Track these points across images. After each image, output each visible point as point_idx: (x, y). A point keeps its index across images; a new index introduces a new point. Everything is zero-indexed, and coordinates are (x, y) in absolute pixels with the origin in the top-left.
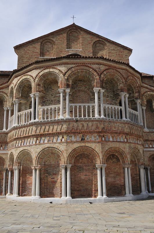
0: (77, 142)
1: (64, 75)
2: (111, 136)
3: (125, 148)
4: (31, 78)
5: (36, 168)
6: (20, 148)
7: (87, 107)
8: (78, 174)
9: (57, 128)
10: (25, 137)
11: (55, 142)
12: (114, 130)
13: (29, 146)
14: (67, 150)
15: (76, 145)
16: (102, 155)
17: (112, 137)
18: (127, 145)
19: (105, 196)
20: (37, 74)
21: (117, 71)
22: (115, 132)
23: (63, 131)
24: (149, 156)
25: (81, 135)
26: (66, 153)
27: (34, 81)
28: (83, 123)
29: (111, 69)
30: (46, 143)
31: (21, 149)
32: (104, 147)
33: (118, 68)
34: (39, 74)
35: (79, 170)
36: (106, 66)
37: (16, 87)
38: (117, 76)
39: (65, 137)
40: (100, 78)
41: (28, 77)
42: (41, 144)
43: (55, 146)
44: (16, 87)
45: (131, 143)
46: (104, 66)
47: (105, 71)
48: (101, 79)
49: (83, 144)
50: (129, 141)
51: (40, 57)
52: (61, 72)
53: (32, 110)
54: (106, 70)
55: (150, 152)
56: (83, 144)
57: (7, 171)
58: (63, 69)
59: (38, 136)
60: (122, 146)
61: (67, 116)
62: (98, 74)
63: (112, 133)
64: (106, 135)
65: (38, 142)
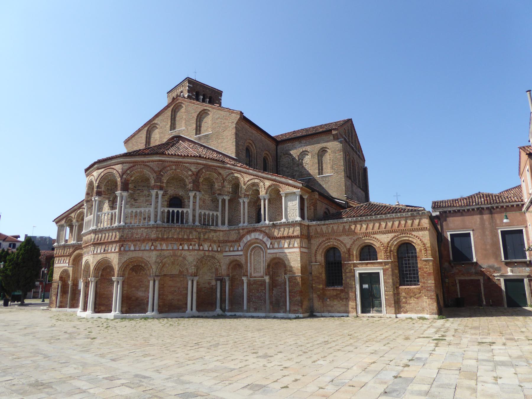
0: (101, 253)
2: (132, 245)
3: (150, 258)
7: (113, 213)
8: (109, 288)
12: (136, 238)
14: (93, 263)
15: (99, 257)
16: (118, 267)
17: (134, 245)
18: (154, 253)
21: (145, 165)
22: (137, 239)
24: (228, 263)
29: (137, 165)
32: (121, 257)
33: (147, 162)
35: (110, 283)
36: (131, 163)
38: (147, 172)
40: (121, 179)
45: (163, 250)
46: (127, 164)
47: (128, 169)
48: (123, 181)
49: (105, 256)
50: (159, 248)
54: (130, 168)
55: (230, 257)
56: (105, 256)
60: (146, 255)
63: (133, 241)
64: (125, 243)
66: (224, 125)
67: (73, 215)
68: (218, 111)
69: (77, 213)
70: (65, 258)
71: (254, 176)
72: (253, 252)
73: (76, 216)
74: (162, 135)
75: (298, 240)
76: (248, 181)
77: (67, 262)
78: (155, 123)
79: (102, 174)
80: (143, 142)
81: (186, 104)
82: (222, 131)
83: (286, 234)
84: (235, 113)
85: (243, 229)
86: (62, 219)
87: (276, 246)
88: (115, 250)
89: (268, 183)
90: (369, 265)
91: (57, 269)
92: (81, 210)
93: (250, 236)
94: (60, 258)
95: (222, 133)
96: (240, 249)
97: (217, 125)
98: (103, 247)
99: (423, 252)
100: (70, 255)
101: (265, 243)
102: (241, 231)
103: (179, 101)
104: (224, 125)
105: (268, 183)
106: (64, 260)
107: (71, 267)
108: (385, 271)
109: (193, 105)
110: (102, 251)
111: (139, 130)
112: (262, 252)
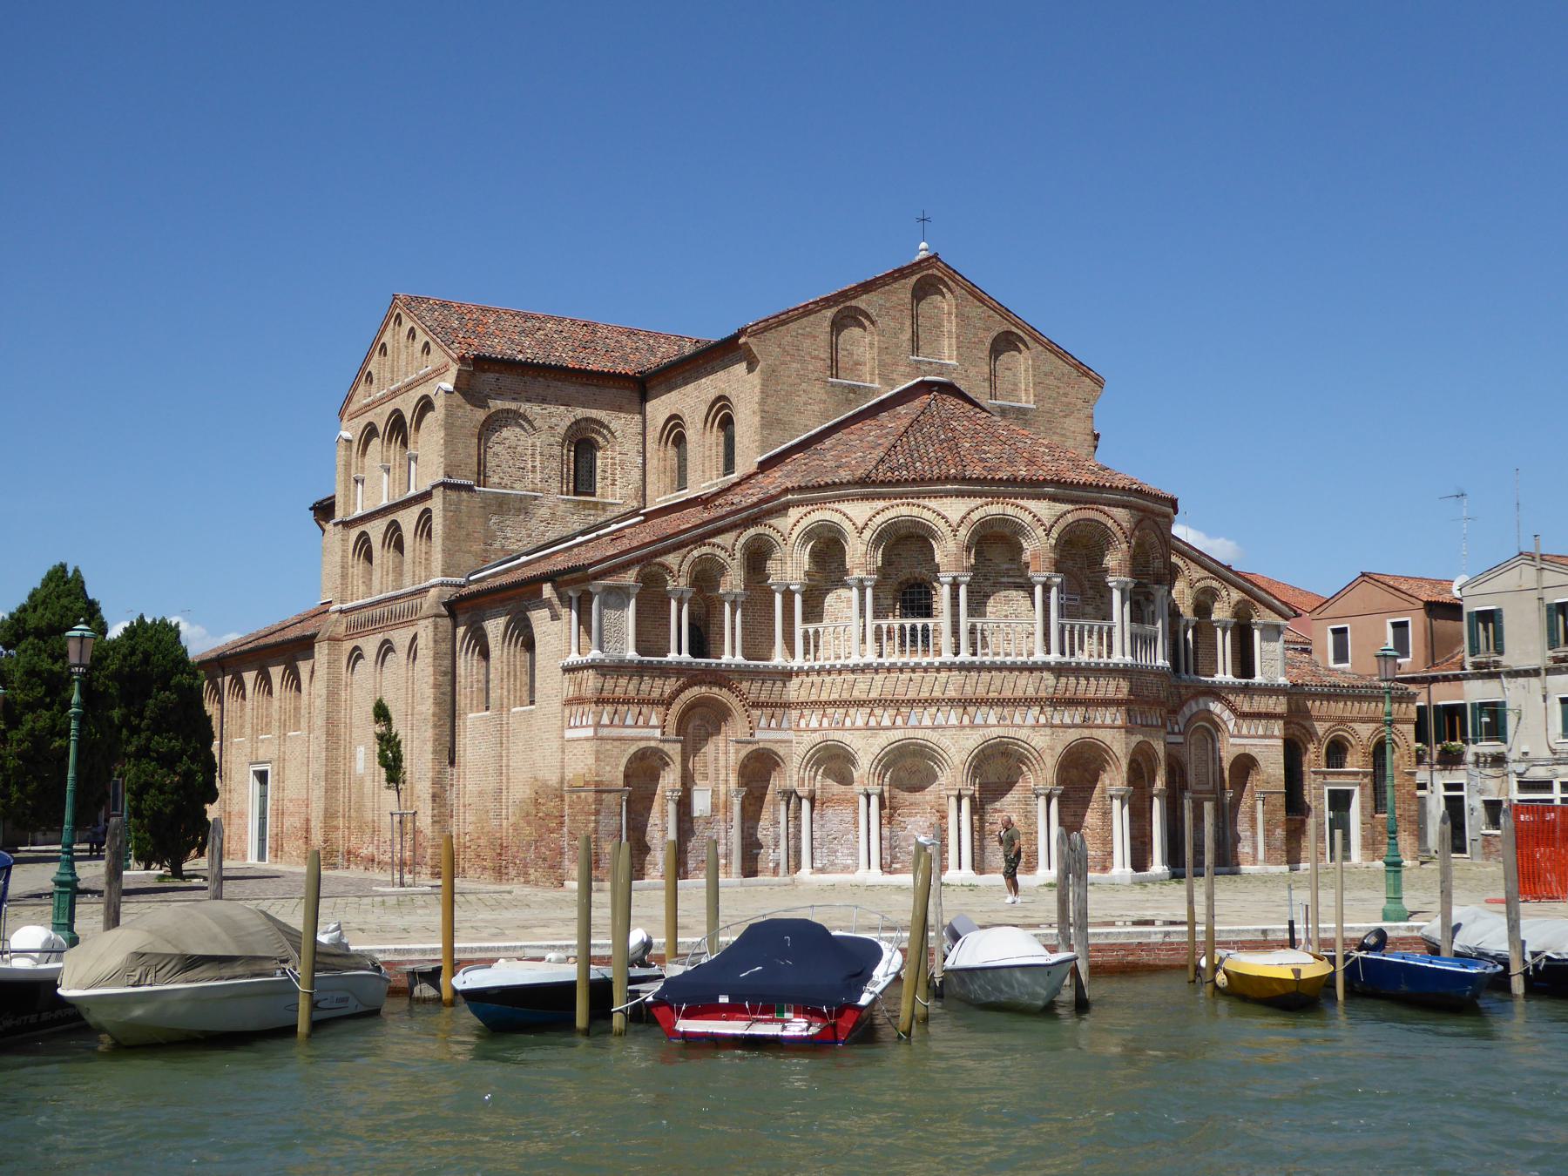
1: (1048, 532)
4: (941, 523)
5: (963, 792)
6: (890, 733)
9: (1026, 685)
10: (911, 703)
11: (1021, 723)
13: (934, 728)
15: (1073, 735)
19: (1129, 869)
20: (963, 513)
23: (1042, 694)
26: (1052, 756)
27: (955, 535)
30: (994, 726)
31: (897, 735)
34: (969, 514)
39: (1048, 710)
41: (927, 515)
42: (979, 726)
43: (1022, 734)
44: (867, 534)
49: (1086, 733)
51: (830, 379)
52: (1039, 520)
56: (1086, 733)
57: (788, 795)
58: (1044, 509)
59: (964, 703)
61: (1054, 657)
62: (1126, 537)
65: (966, 720)
66: (1064, 399)
67: (671, 560)
68: (1048, 353)
69: (690, 558)
70: (645, 710)
71: (1209, 571)
72: (1194, 737)
73: (685, 568)
74: (888, 359)
75: (1281, 723)
76: (1199, 581)
77: (654, 721)
78: (856, 309)
79: (1070, 518)
80: (822, 356)
81: (958, 290)
82: (1061, 414)
83: (1263, 710)
84: (1092, 379)
85: (1187, 687)
86: (625, 567)
87: (1245, 731)
88: (1113, 721)
89: (1236, 595)
90: (1341, 777)
91: (608, 747)
92: (705, 550)
93: (1197, 703)
94: (622, 708)
95: (1059, 420)
96: (1176, 730)
97: (1049, 393)
98: (1082, 710)
99: (1406, 759)
100: (667, 703)
101: (1225, 723)
102: (1183, 691)
103: (935, 272)
104: (1066, 400)
105: (1236, 595)
106: (640, 713)
107: (675, 741)
108: (1363, 787)
109: (978, 303)
110: (1078, 720)
111: (806, 311)
112: (1210, 741)
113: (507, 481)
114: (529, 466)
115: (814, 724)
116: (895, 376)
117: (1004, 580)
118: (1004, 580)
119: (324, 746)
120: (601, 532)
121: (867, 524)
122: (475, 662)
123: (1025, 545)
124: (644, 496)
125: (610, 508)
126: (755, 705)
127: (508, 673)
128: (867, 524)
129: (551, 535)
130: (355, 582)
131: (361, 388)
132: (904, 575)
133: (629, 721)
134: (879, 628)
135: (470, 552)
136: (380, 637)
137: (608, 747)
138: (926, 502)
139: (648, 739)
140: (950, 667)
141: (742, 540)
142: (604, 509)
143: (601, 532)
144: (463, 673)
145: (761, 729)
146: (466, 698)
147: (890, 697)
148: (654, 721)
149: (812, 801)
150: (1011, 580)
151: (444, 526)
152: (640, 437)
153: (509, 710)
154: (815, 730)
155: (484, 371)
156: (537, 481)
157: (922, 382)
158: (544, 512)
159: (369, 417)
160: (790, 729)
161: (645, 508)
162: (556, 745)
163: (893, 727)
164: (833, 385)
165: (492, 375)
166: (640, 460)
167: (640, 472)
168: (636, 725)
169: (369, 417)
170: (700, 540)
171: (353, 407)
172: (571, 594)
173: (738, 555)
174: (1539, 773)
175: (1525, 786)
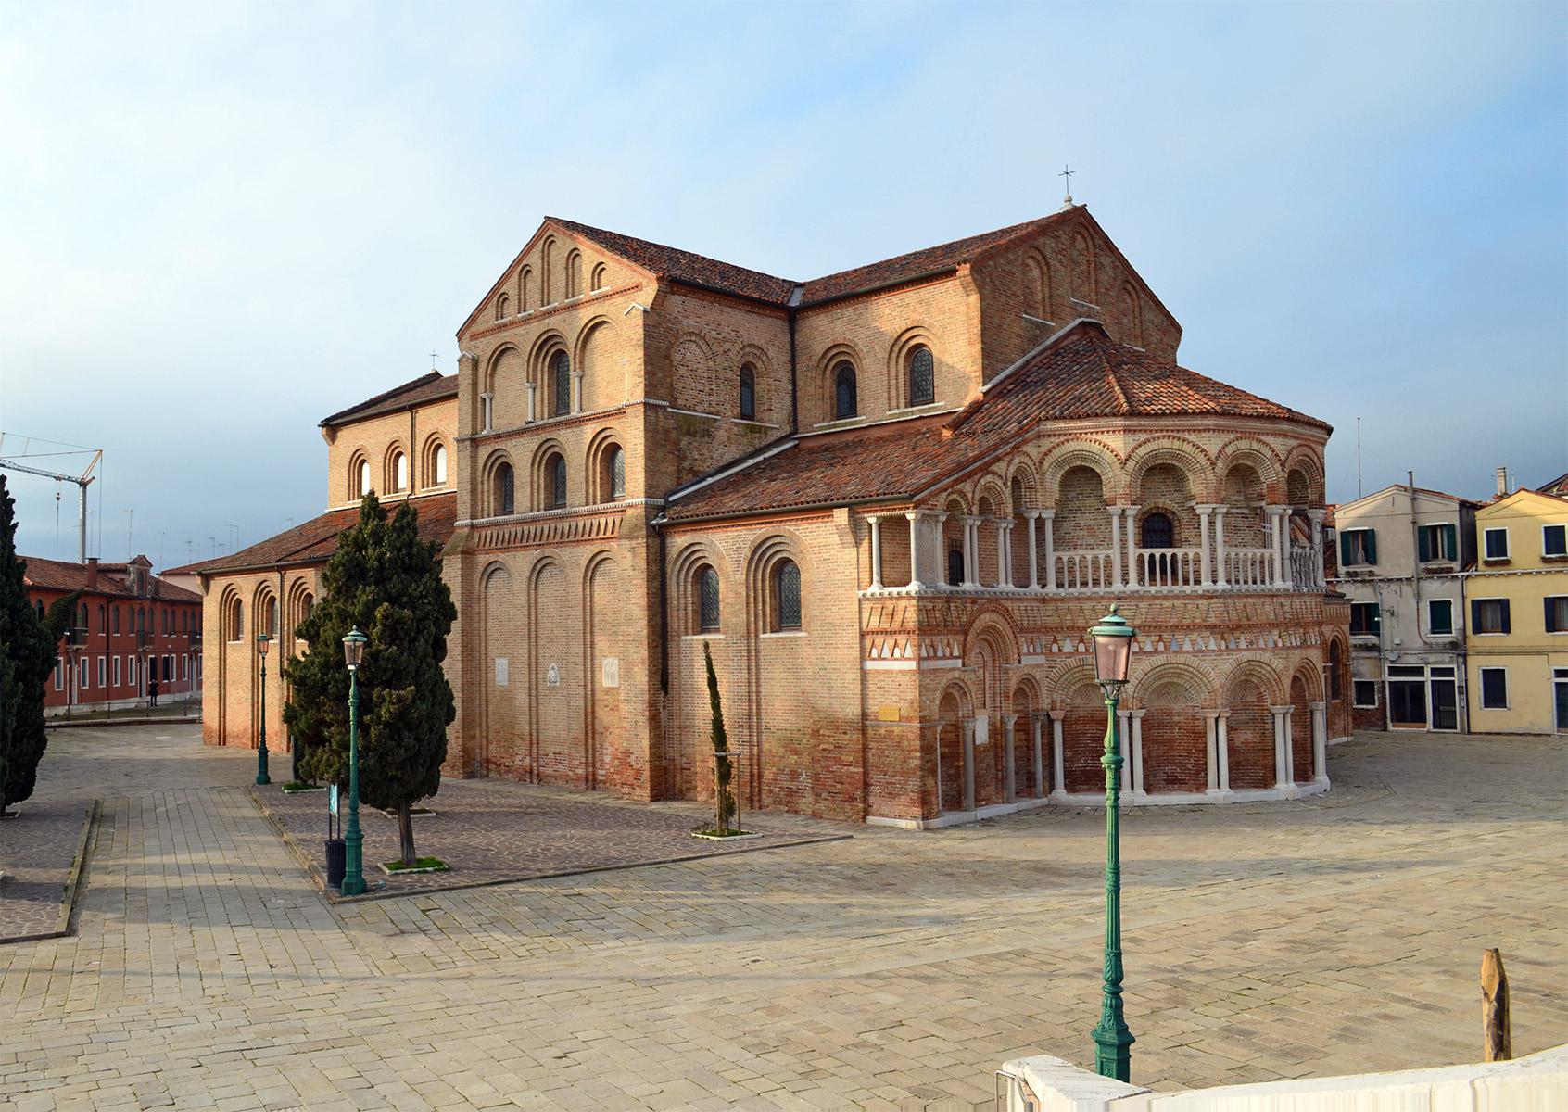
4: (1201, 457)
10: (1176, 628)
14: (1287, 668)
15: (1297, 656)
25: (1302, 631)
28: (1306, 599)
31: (1160, 659)
37: (1131, 465)
41: (1188, 448)
42: (1233, 650)
43: (1266, 657)
52: (1277, 455)
53: (1204, 553)
58: (1280, 445)
61: (1289, 585)
65: (1223, 647)
67: (967, 487)
73: (977, 497)
77: (956, 653)
91: (928, 681)
92: (989, 478)
94: (936, 639)
109: (1109, 253)
113: (691, 403)
114: (707, 390)
115: (1068, 648)
116: (1063, 316)
117: (1234, 511)
118: (1234, 511)
119: (459, 658)
120: (767, 455)
121: (1130, 456)
122: (689, 586)
123: (1262, 479)
124: (795, 421)
125: (770, 433)
126: (1023, 631)
127: (755, 598)
128: (1130, 456)
129: (728, 458)
130: (486, 499)
131: (491, 310)
132: (1149, 504)
133: (940, 654)
134: (1141, 556)
135: (667, 473)
136: (537, 553)
137: (928, 681)
138: (1186, 435)
139: (954, 669)
140: (1209, 596)
141: (1012, 469)
142: (766, 433)
143: (767, 455)
144: (674, 594)
145: (1025, 655)
146: (679, 619)
147: (1154, 624)
148: (956, 653)
149: (1063, 721)
150: (1238, 511)
151: (645, 446)
152: (789, 367)
153: (757, 636)
154: (1070, 655)
155: (673, 294)
156: (714, 404)
157: (1082, 322)
158: (721, 435)
159: (505, 336)
160: (1042, 653)
161: (796, 433)
162: (857, 675)
163: (1156, 651)
164: (1026, 320)
165: (679, 298)
166: (790, 387)
167: (790, 399)
168: (941, 658)
169: (505, 336)
170: (985, 469)
171: (475, 328)
172: (872, 520)
173: (1009, 483)
174: (1411, 661)
175: (1393, 671)
